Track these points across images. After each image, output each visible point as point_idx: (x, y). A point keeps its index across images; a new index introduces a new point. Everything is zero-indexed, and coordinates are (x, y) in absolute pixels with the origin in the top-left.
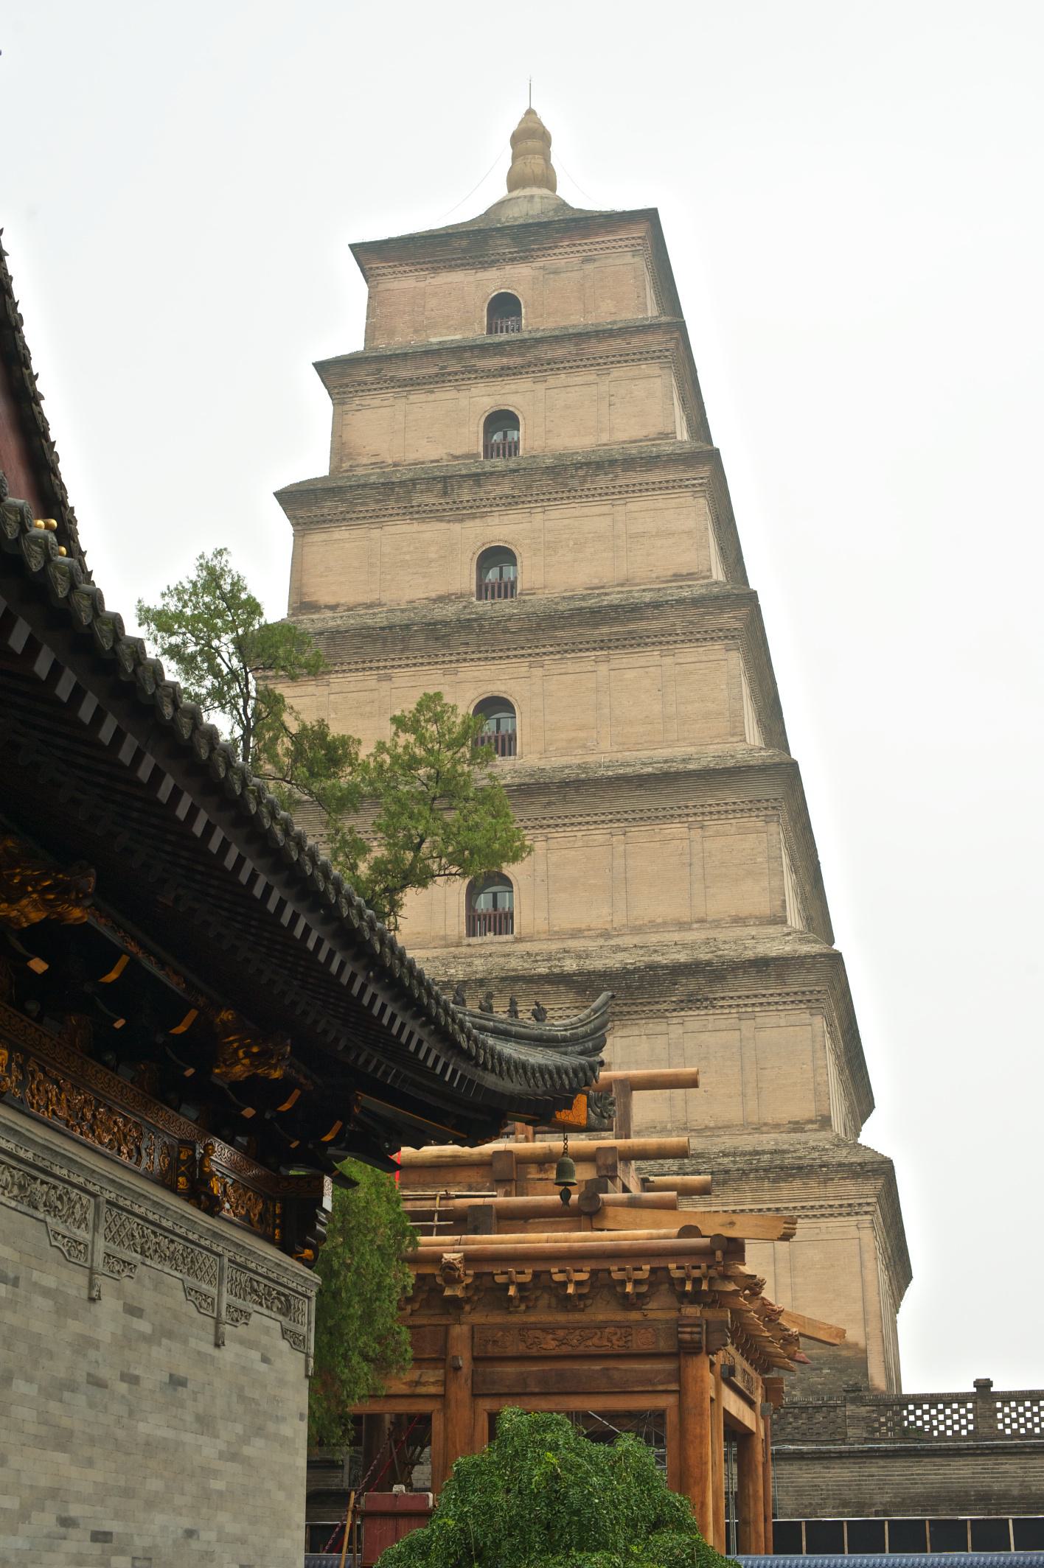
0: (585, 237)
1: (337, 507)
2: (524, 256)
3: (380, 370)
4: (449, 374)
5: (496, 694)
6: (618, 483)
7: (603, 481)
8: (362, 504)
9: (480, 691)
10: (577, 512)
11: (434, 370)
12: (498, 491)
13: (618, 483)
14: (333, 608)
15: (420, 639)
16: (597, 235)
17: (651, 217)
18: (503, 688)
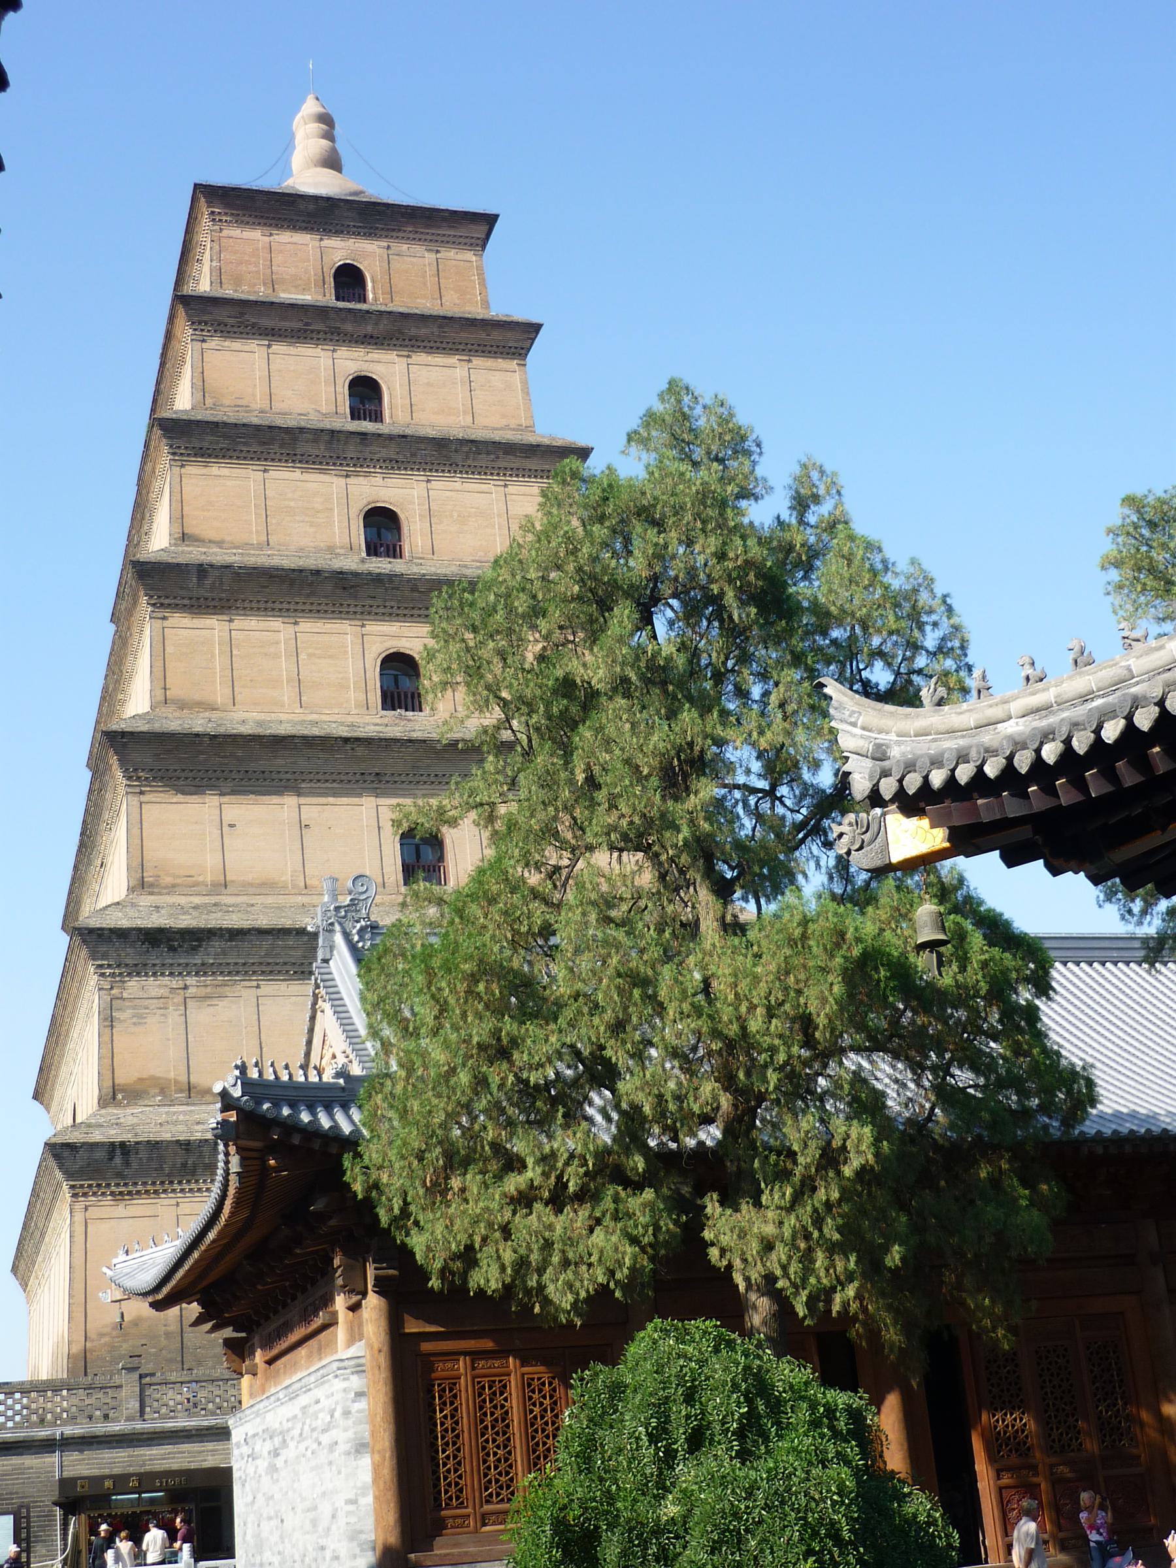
0: (428, 226)
1: (217, 443)
2: (370, 232)
3: (242, 314)
4: (312, 331)
5: (402, 650)
6: (496, 465)
7: (483, 460)
8: (245, 444)
9: (388, 644)
10: (458, 485)
11: (300, 325)
12: (384, 453)
13: (496, 465)
14: (220, 544)
15: (328, 587)
16: (439, 227)
18: (408, 645)
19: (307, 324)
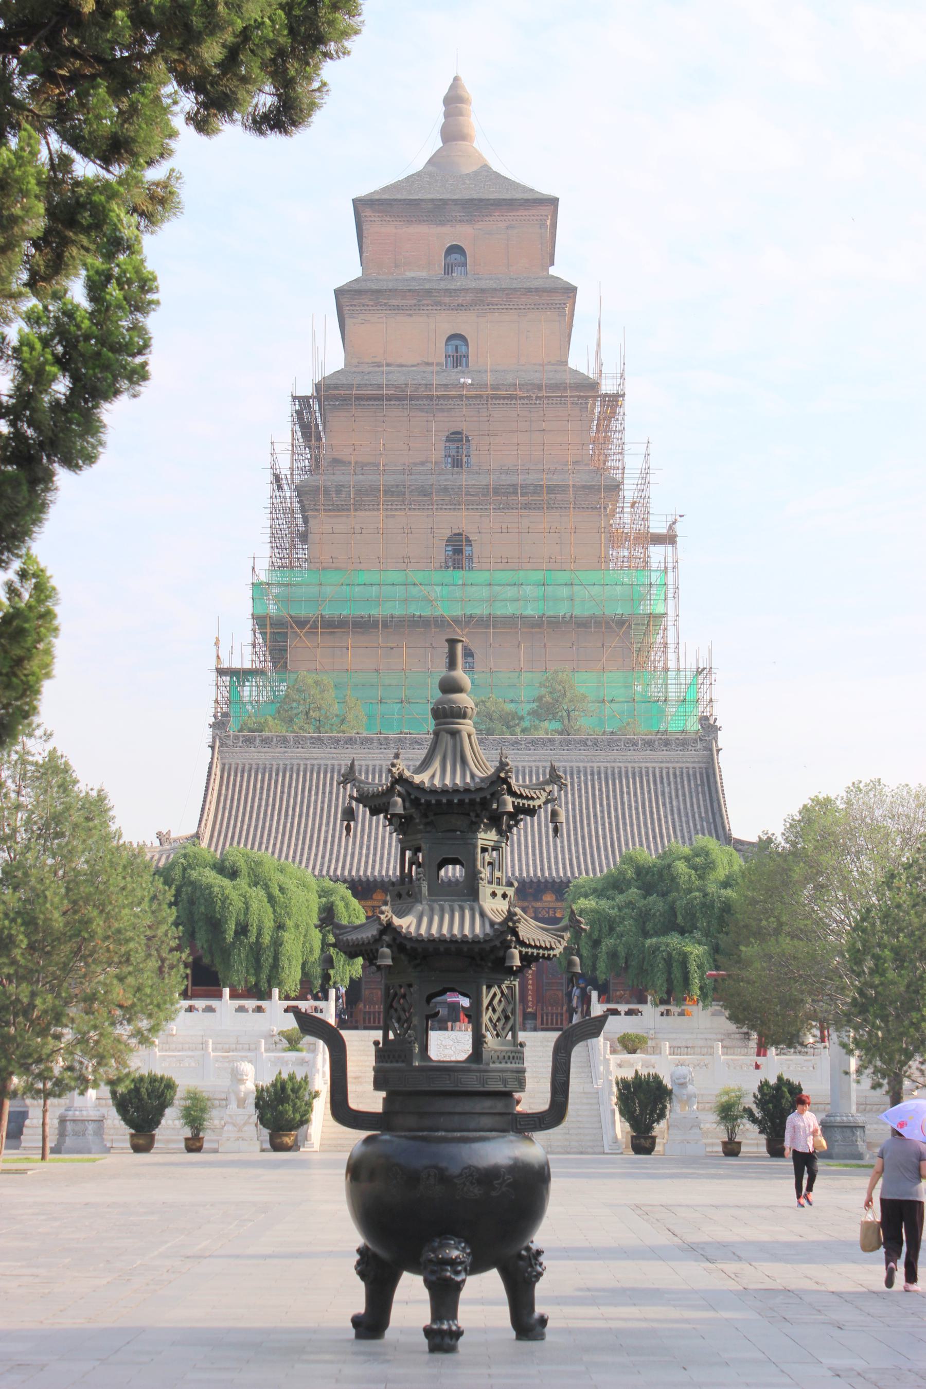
2: (469, 222)
11: (414, 302)
16: (517, 210)
17: (553, 202)
19: (419, 301)
